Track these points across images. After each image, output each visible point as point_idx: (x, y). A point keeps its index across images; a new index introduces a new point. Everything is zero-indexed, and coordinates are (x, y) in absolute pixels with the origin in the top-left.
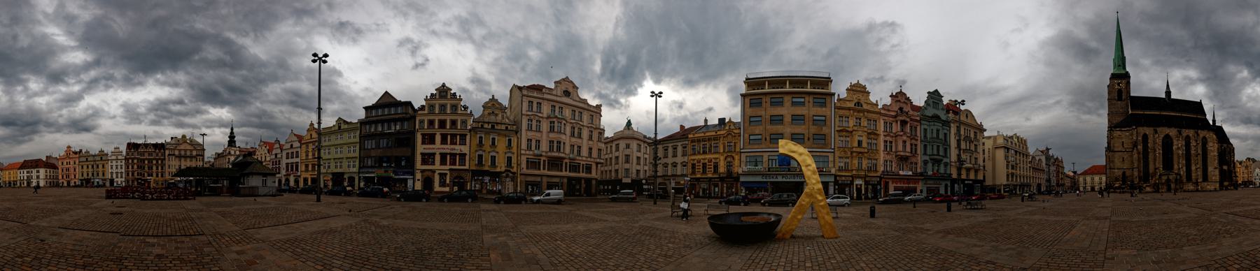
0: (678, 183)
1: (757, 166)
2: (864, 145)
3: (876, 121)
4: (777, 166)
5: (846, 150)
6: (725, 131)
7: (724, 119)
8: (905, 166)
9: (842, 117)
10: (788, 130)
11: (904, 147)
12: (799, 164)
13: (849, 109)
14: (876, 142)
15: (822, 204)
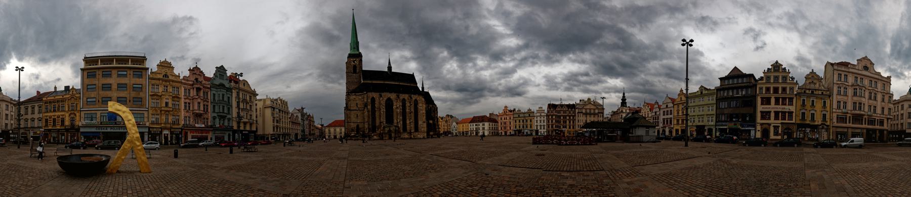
0: (35, 133)
1: (92, 120)
2: (170, 105)
5: (157, 109)
6: (69, 96)
7: (69, 87)
8: (199, 121)
10: (115, 94)
11: (199, 106)
12: (122, 119)
13: (159, 79)
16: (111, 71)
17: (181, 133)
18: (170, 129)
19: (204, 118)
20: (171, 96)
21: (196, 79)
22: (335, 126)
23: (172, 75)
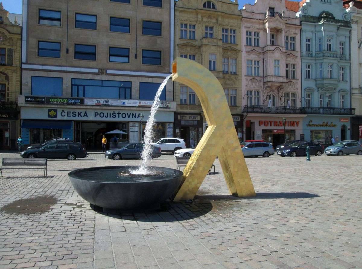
3: (234, 31)
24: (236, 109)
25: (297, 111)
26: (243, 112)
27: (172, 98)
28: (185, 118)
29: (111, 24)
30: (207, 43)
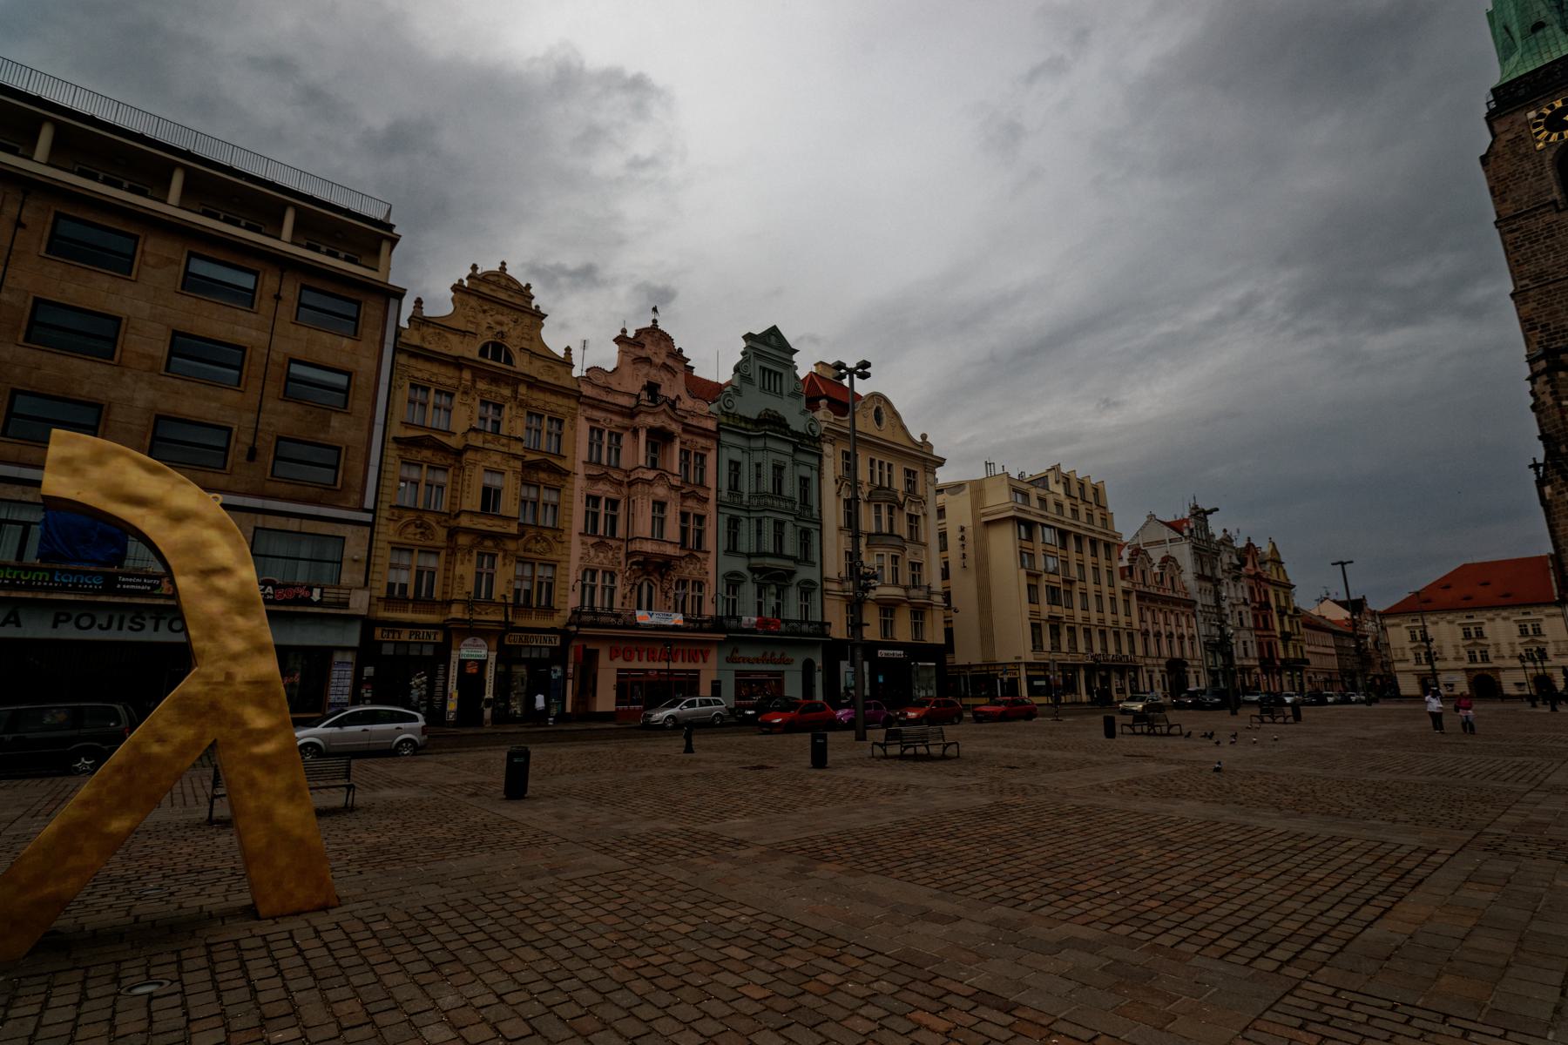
2: (508, 505)
3: (560, 422)
4: (31, 557)
8: (657, 594)
9: (426, 389)
11: (659, 522)
13: (458, 363)
14: (554, 498)
15: (268, 747)
16: (136, 238)
17: (559, 656)
18: (495, 634)
19: (684, 583)
20: (515, 457)
21: (652, 388)
22: (1468, 605)
23: (533, 354)
24: (552, 615)
25: (706, 625)
26: (569, 624)
27: (362, 579)
28: (396, 635)
29: (171, 353)
30: (480, 445)
